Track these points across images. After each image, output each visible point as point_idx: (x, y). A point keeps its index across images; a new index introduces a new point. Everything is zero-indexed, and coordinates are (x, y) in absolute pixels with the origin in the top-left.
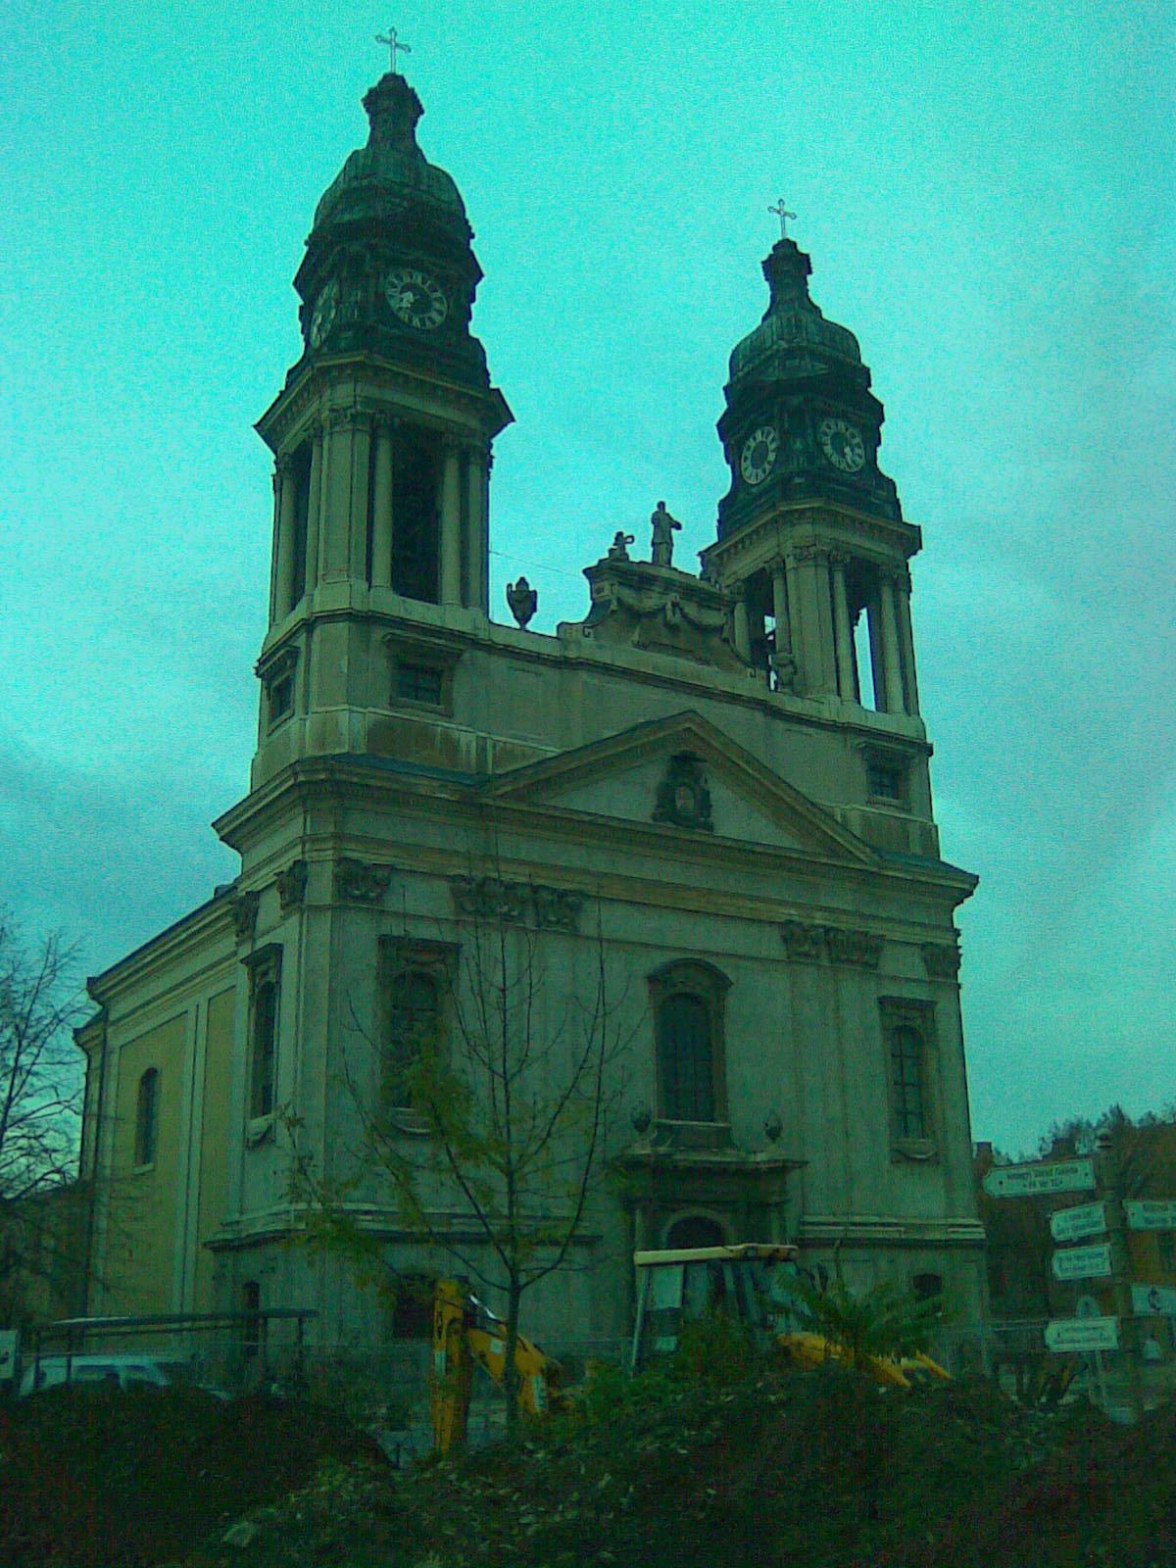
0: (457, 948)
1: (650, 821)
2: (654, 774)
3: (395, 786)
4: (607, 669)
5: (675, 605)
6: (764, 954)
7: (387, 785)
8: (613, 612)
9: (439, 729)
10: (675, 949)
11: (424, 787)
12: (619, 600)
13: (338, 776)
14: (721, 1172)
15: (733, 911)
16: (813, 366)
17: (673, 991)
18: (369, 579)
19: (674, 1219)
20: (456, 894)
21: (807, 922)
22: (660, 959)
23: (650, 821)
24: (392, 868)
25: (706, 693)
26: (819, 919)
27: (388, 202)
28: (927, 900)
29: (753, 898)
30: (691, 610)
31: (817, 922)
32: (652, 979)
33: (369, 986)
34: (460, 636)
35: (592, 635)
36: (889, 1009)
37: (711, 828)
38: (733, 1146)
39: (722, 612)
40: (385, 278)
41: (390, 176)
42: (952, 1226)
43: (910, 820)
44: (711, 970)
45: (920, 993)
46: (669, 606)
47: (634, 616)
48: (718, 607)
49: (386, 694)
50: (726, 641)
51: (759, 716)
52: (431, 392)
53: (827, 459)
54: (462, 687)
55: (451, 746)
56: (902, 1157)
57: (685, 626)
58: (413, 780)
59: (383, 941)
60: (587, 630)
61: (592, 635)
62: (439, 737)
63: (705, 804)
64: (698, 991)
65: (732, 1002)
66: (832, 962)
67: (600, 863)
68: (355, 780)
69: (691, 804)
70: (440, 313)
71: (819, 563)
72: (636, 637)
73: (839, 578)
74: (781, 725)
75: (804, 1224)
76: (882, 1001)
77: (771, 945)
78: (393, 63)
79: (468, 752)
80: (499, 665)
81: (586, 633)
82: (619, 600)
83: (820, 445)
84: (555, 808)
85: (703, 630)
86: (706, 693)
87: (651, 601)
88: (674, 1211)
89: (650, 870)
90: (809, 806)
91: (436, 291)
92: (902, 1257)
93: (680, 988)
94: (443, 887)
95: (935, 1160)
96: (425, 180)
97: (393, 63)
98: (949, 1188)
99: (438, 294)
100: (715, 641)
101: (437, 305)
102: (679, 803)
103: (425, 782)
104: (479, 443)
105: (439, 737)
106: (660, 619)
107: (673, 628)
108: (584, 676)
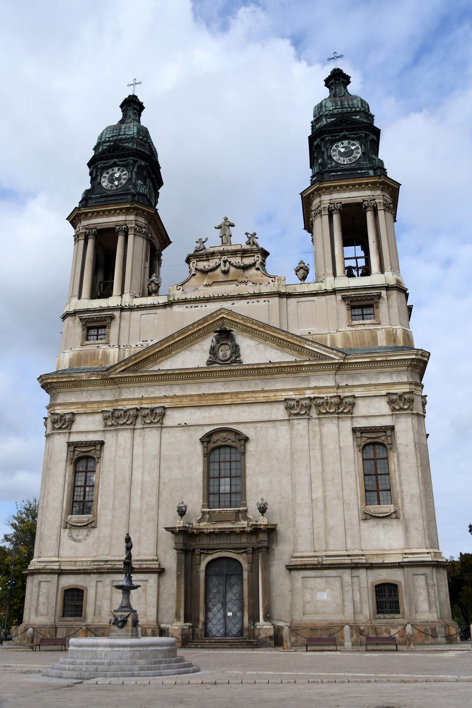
0: (102, 443)
1: (206, 366)
2: (208, 342)
3: (73, 379)
4: (185, 301)
5: (225, 262)
6: (274, 418)
7: (69, 379)
8: (194, 275)
9: (101, 350)
10: (216, 424)
11: (84, 376)
12: (196, 269)
13: (49, 381)
14: (232, 533)
15: (252, 400)
16: (327, 121)
17: (214, 445)
18: (79, 298)
19: (209, 558)
20: (105, 419)
21: (298, 397)
22: (208, 430)
23: (206, 366)
24: (74, 414)
25: (241, 297)
26: (309, 394)
27: (104, 146)
28: (388, 369)
29: (263, 391)
30: (236, 260)
31: (307, 396)
32: (202, 441)
33: (63, 464)
34: (114, 309)
35: (181, 289)
36: (359, 434)
37: (240, 362)
38: (246, 518)
39: (256, 256)
40: (101, 175)
41: (108, 136)
42: (406, 554)
43: (378, 329)
44: (237, 433)
45: (387, 422)
46: (222, 263)
47: (205, 272)
48: (253, 255)
49: (79, 341)
50: (258, 269)
51: (276, 300)
52: (110, 213)
53: (336, 162)
54: (114, 330)
55: (106, 356)
56: (367, 517)
57: (232, 269)
58: (79, 375)
59: (69, 444)
60: (179, 287)
61: (181, 289)
62: (100, 354)
63: (236, 350)
64: (229, 443)
65: (250, 447)
66: (319, 414)
67: (177, 391)
68: (55, 381)
69: (229, 353)
70: (124, 179)
71: (323, 214)
72: (205, 283)
73: (336, 218)
74: (292, 301)
75: (294, 557)
76: (354, 430)
77: (280, 412)
78: (134, 90)
79: (114, 357)
80: (136, 314)
81: (179, 289)
82: (196, 269)
83: (330, 157)
84: (154, 371)
85: (246, 268)
86: (241, 297)
87: (212, 263)
88: (210, 554)
89: (206, 388)
90: (295, 338)
91: (124, 171)
92: (362, 573)
93: (219, 443)
94: (99, 418)
95: (394, 516)
96: (123, 130)
97: (134, 90)
98: (406, 530)
99: (125, 172)
100: (253, 271)
101: (124, 177)
102: (221, 354)
103: (84, 374)
104: (134, 225)
105: (100, 354)
106: (218, 271)
107: (226, 272)
108: (176, 308)
